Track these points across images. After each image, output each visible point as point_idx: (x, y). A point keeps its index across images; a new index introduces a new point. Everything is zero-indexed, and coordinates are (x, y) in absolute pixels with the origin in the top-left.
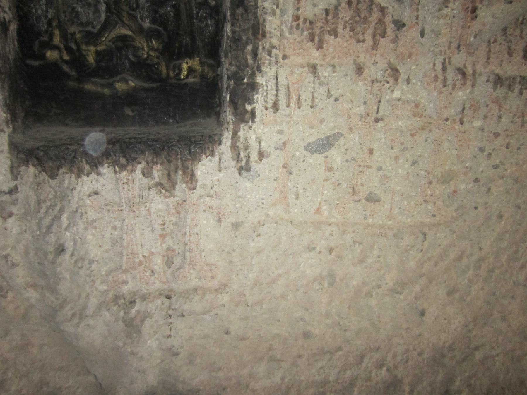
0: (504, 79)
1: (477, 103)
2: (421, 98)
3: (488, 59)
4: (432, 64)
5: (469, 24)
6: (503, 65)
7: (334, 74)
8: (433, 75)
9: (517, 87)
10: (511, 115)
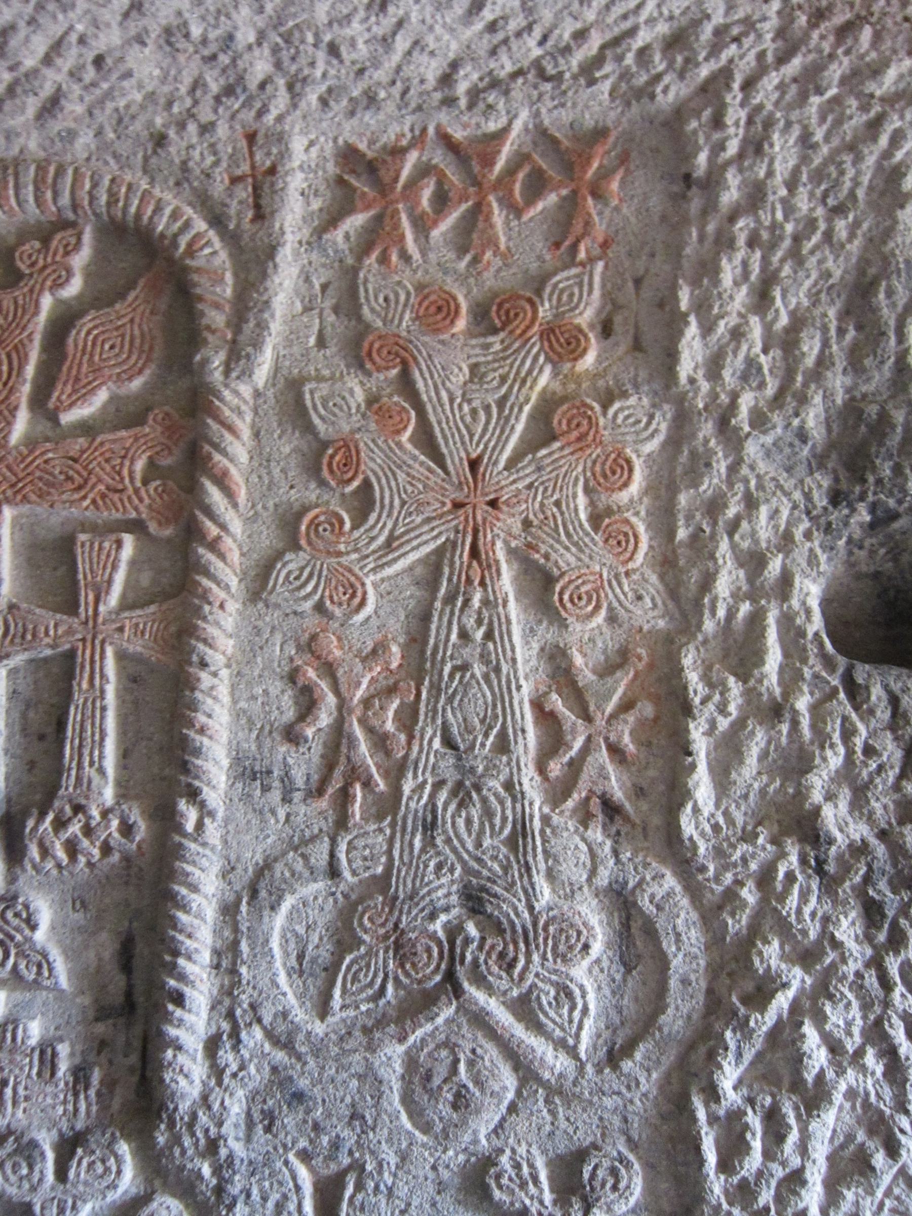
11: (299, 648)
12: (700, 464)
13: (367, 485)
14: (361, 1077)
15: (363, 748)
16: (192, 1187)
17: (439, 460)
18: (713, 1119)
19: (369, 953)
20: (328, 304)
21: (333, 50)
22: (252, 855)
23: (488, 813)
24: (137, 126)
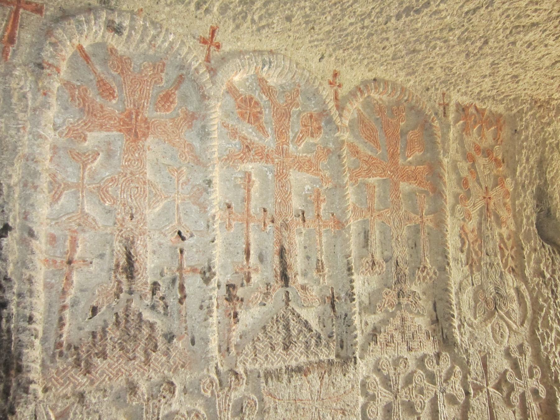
7: (105, 399)
11: (461, 229)
12: (519, 196)
13: (469, 190)
14: (485, 332)
15: (474, 255)
16: (462, 362)
17: (481, 186)
18: (539, 335)
19: (482, 303)
20: (457, 142)
21: (468, 82)
22: (458, 281)
23: (496, 270)
24: (423, 84)
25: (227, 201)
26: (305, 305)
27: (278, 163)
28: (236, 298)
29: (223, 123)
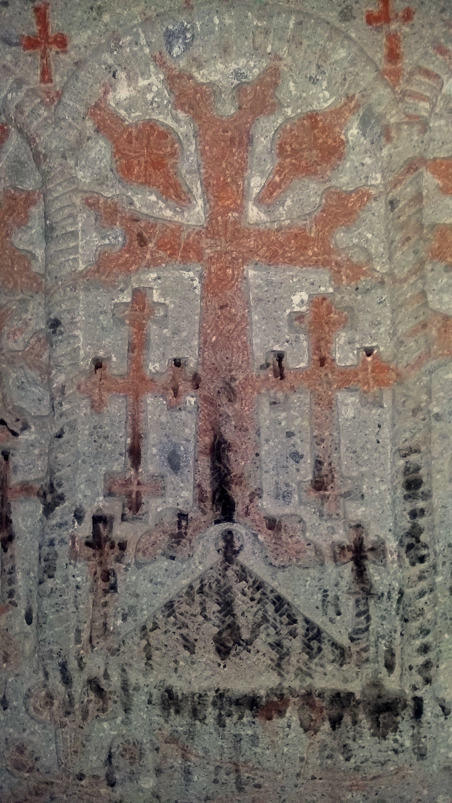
0: (180, 697)
1: (134, 744)
2: (32, 733)
3: (149, 658)
4: (41, 674)
5: (102, 601)
6: (180, 669)
8: (43, 693)
9: (211, 713)
10: (211, 768)
25: (101, 353)
26: (277, 563)
27: (211, 258)
28: (108, 544)
29: (87, 199)
